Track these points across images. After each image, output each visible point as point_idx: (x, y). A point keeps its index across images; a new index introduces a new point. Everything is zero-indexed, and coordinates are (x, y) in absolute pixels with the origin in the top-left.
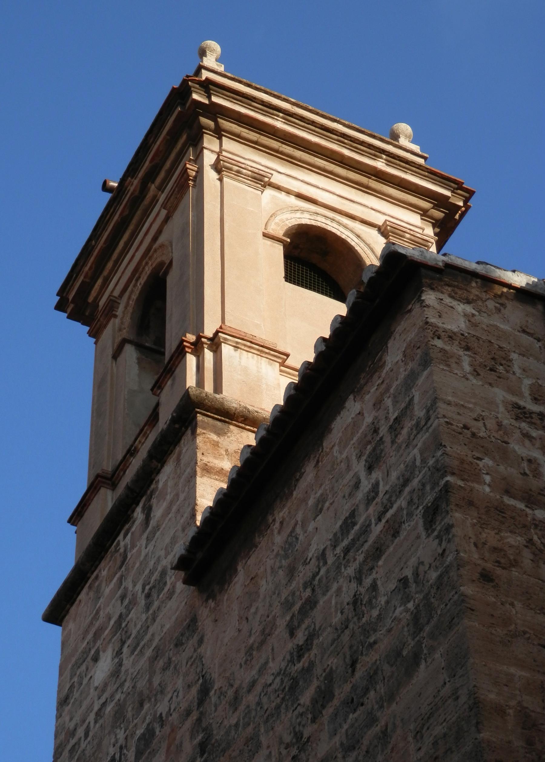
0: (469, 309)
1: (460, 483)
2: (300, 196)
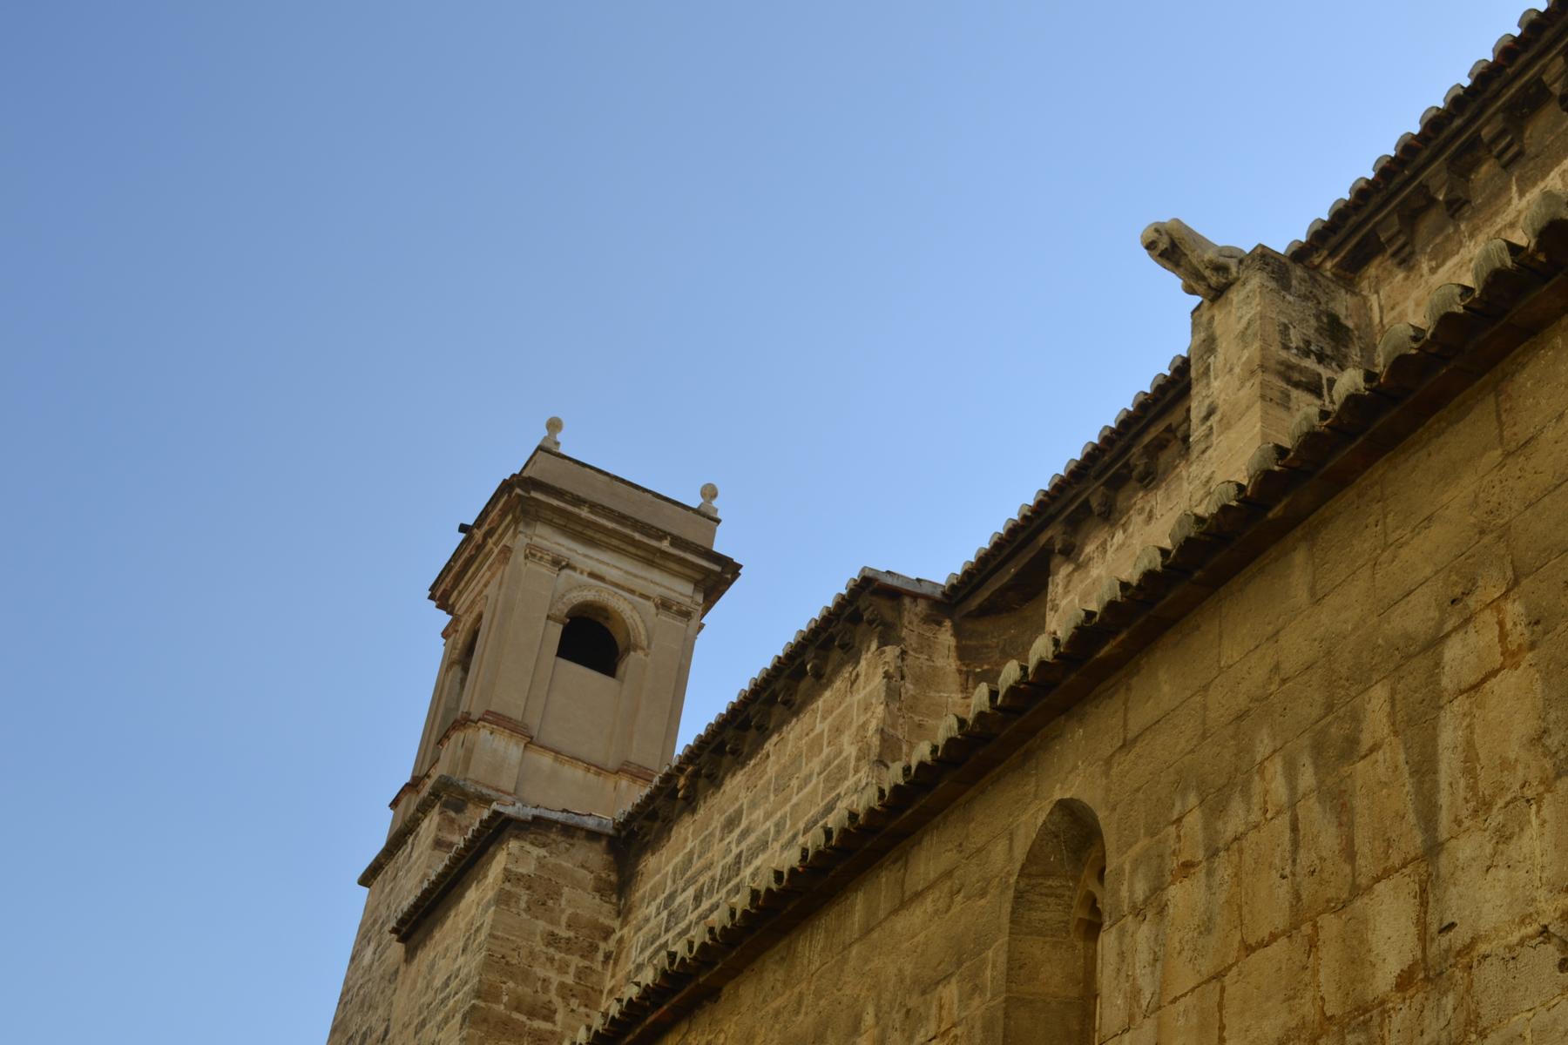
0: (543, 852)
1: (483, 1004)
2: (592, 575)
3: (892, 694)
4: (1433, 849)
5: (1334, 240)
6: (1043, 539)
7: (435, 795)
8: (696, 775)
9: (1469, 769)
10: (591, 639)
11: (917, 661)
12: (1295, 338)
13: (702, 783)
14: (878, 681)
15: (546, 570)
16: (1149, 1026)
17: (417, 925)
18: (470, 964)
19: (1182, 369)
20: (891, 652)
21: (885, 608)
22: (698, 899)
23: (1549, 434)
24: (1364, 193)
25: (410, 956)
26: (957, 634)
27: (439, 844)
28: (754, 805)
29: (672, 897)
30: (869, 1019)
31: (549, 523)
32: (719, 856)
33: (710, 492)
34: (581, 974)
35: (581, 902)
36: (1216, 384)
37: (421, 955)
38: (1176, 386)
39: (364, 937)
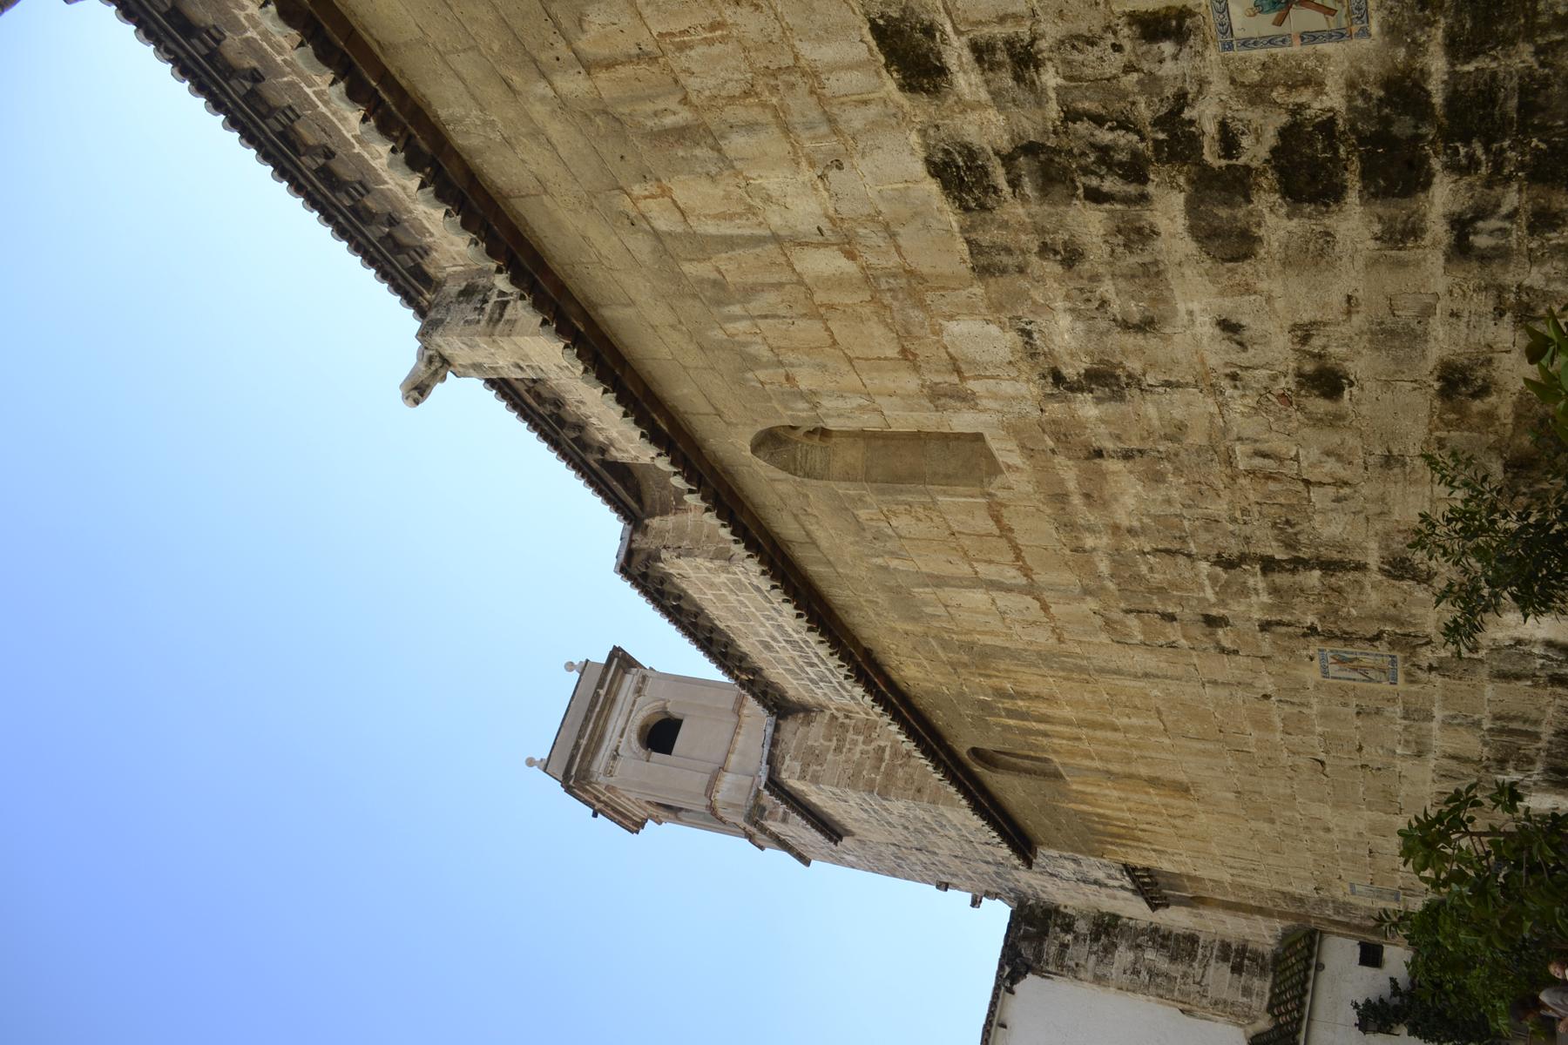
3: (689, 553)
4: (776, 238)
5: (413, 293)
6: (595, 466)
7: (755, 824)
8: (739, 668)
9: (731, 217)
10: (661, 735)
11: (669, 539)
12: (474, 316)
13: (744, 665)
14: (682, 562)
15: (620, 764)
16: (879, 400)
17: (831, 830)
18: (854, 797)
19: (491, 383)
20: (664, 554)
21: (638, 559)
22: (812, 665)
23: (534, 168)
24: (384, 275)
25: (850, 833)
26: (652, 515)
27: (784, 820)
28: (757, 634)
29: (811, 680)
30: (879, 561)
31: (590, 763)
32: (786, 653)
33: (570, 666)
34: (857, 732)
35: (815, 735)
36: (501, 363)
37: (849, 827)
38: (503, 387)
39: (839, 861)
